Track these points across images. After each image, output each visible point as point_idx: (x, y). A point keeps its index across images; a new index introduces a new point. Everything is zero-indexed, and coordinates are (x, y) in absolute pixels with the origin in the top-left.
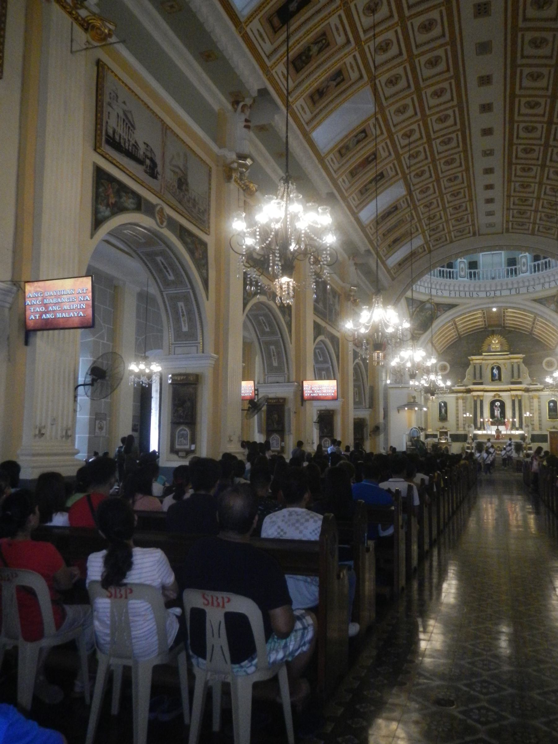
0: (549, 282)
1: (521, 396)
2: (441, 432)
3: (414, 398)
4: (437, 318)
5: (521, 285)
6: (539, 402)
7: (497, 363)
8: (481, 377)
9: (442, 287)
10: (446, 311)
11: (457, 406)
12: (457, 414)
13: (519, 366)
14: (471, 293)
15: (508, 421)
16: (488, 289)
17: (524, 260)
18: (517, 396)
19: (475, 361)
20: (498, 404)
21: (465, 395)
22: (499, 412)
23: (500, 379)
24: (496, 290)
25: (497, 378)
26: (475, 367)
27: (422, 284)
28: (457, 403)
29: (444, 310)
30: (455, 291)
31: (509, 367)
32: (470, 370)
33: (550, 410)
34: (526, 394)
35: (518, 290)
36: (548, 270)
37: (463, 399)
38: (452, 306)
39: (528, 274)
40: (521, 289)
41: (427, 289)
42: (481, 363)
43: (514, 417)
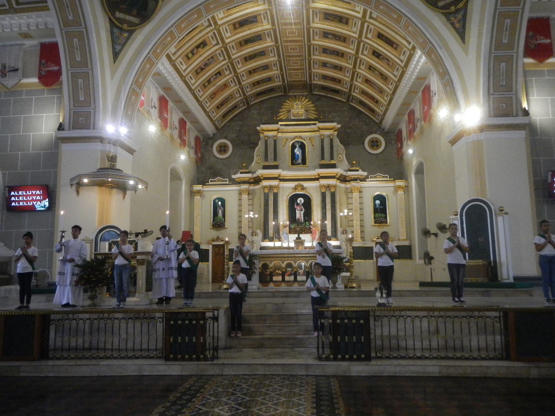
1: (335, 186)
2: (214, 246)
3: (113, 159)
7: (300, 137)
8: (275, 159)
11: (240, 205)
13: (331, 140)
15: (315, 226)
18: (328, 187)
19: (266, 133)
20: (301, 200)
21: (252, 187)
22: (302, 212)
23: (304, 162)
25: (300, 161)
26: (266, 141)
28: (240, 200)
31: (317, 143)
32: (259, 149)
33: (376, 211)
34: (343, 185)
37: (249, 194)
42: (276, 136)
43: (324, 218)
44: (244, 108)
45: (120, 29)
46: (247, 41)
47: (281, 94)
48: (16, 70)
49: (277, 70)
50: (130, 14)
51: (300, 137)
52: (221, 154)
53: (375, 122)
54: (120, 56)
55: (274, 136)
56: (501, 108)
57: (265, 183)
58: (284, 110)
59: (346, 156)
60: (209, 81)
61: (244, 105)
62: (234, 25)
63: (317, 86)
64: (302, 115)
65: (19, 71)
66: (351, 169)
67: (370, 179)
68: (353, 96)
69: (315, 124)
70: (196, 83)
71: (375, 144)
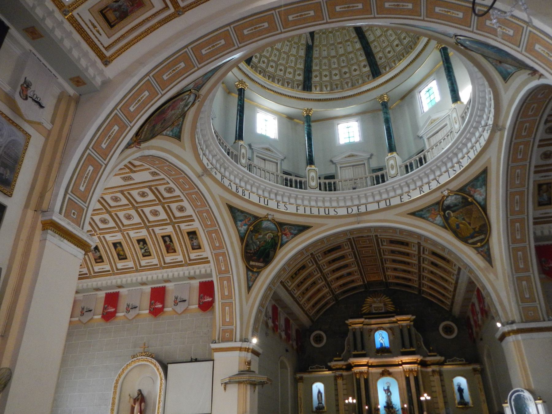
0: (429, 183)
4: (282, 245)
5: (392, 194)
6: (442, 380)
8: (363, 348)
9: (286, 200)
10: (296, 235)
11: (336, 390)
12: (337, 400)
14: (327, 210)
16: (349, 203)
17: (392, 162)
18: (411, 371)
24: (360, 205)
26: (354, 334)
27: (254, 190)
28: (336, 385)
29: (291, 234)
30: (305, 206)
34: (424, 369)
35: (388, 201)
36: (424, 165)
37: (343, 380)
38: (303, 228)
39: (399, 177)
40: (391, 200)
41: (262, 199)
44: (334, 302)
45: (252, 271)
46: (334, 260)
47: (363, 290)
48: (185, 301)
49: (358, 275)
50: (259, 262)
51: (382, 327)
52: (317, 344)
53: (445, 310)
54: (252, 288)
55: (360, 329)
56: (530, 315)
57: (356, 370)
58: (367, 305)
59: (424, 343)
60: (307, 290)
61: (334, 301)
62: (325, 252)
63: (391, 283)
64: (382, 310)
65: (186, 302)
66: (429, 354)
67: (448, 363)
68: (423, 291)
69: (393, 316)
70: (297, 293)
71: (448, 330)
